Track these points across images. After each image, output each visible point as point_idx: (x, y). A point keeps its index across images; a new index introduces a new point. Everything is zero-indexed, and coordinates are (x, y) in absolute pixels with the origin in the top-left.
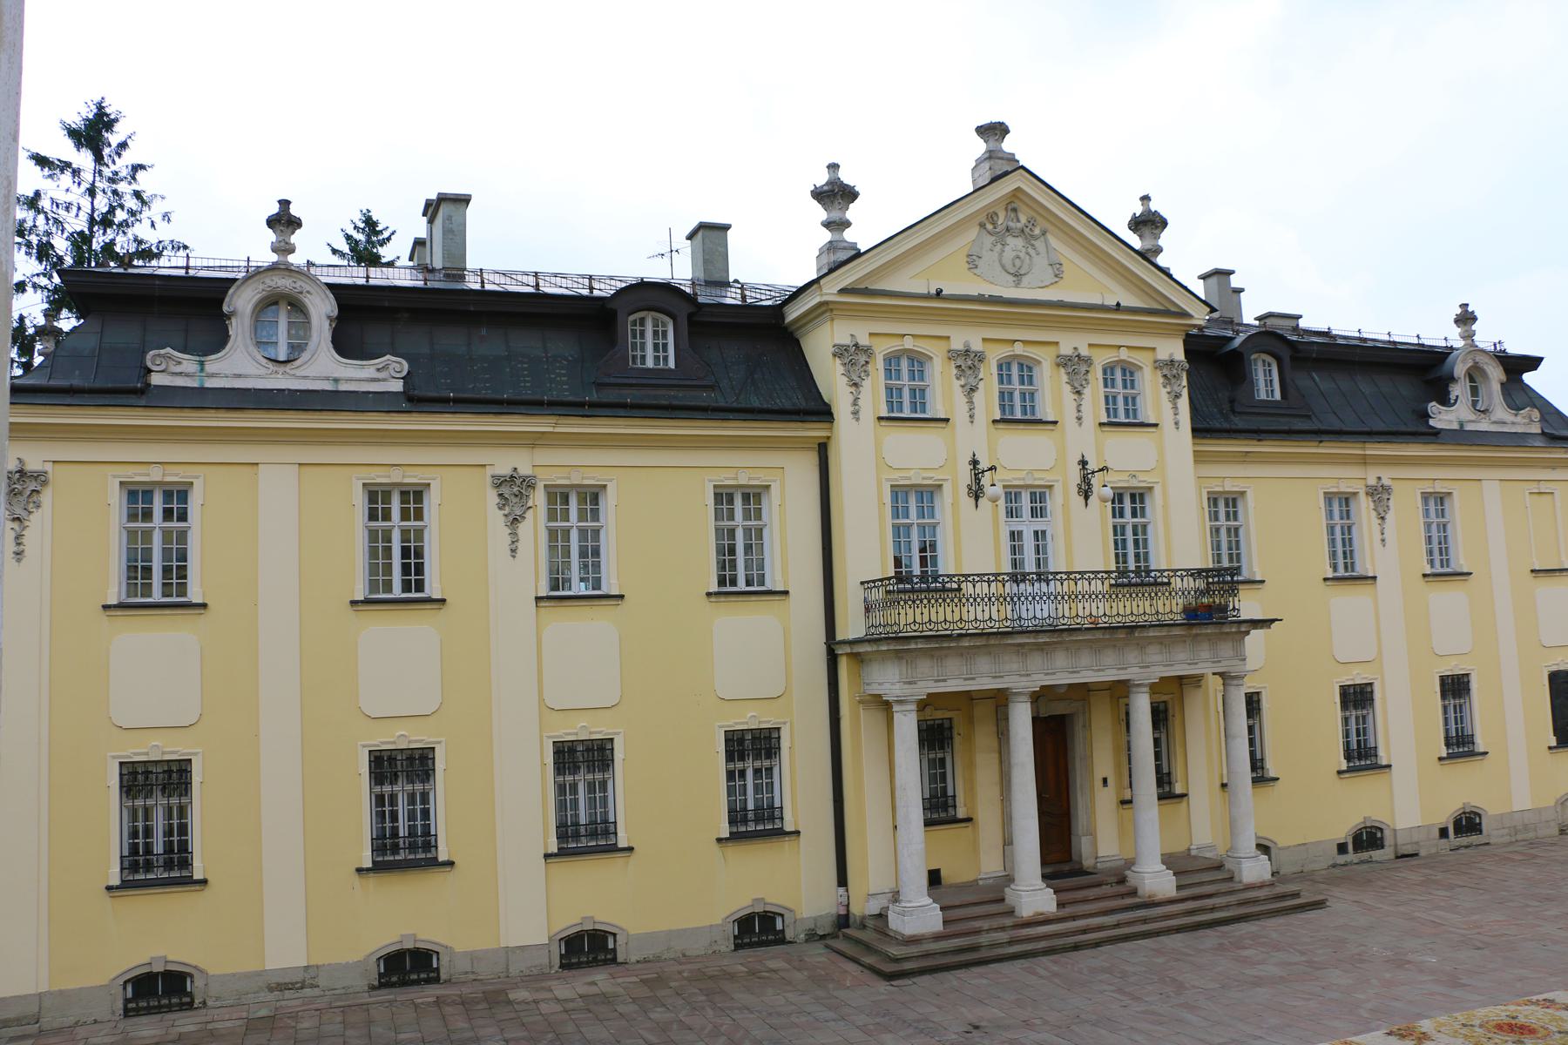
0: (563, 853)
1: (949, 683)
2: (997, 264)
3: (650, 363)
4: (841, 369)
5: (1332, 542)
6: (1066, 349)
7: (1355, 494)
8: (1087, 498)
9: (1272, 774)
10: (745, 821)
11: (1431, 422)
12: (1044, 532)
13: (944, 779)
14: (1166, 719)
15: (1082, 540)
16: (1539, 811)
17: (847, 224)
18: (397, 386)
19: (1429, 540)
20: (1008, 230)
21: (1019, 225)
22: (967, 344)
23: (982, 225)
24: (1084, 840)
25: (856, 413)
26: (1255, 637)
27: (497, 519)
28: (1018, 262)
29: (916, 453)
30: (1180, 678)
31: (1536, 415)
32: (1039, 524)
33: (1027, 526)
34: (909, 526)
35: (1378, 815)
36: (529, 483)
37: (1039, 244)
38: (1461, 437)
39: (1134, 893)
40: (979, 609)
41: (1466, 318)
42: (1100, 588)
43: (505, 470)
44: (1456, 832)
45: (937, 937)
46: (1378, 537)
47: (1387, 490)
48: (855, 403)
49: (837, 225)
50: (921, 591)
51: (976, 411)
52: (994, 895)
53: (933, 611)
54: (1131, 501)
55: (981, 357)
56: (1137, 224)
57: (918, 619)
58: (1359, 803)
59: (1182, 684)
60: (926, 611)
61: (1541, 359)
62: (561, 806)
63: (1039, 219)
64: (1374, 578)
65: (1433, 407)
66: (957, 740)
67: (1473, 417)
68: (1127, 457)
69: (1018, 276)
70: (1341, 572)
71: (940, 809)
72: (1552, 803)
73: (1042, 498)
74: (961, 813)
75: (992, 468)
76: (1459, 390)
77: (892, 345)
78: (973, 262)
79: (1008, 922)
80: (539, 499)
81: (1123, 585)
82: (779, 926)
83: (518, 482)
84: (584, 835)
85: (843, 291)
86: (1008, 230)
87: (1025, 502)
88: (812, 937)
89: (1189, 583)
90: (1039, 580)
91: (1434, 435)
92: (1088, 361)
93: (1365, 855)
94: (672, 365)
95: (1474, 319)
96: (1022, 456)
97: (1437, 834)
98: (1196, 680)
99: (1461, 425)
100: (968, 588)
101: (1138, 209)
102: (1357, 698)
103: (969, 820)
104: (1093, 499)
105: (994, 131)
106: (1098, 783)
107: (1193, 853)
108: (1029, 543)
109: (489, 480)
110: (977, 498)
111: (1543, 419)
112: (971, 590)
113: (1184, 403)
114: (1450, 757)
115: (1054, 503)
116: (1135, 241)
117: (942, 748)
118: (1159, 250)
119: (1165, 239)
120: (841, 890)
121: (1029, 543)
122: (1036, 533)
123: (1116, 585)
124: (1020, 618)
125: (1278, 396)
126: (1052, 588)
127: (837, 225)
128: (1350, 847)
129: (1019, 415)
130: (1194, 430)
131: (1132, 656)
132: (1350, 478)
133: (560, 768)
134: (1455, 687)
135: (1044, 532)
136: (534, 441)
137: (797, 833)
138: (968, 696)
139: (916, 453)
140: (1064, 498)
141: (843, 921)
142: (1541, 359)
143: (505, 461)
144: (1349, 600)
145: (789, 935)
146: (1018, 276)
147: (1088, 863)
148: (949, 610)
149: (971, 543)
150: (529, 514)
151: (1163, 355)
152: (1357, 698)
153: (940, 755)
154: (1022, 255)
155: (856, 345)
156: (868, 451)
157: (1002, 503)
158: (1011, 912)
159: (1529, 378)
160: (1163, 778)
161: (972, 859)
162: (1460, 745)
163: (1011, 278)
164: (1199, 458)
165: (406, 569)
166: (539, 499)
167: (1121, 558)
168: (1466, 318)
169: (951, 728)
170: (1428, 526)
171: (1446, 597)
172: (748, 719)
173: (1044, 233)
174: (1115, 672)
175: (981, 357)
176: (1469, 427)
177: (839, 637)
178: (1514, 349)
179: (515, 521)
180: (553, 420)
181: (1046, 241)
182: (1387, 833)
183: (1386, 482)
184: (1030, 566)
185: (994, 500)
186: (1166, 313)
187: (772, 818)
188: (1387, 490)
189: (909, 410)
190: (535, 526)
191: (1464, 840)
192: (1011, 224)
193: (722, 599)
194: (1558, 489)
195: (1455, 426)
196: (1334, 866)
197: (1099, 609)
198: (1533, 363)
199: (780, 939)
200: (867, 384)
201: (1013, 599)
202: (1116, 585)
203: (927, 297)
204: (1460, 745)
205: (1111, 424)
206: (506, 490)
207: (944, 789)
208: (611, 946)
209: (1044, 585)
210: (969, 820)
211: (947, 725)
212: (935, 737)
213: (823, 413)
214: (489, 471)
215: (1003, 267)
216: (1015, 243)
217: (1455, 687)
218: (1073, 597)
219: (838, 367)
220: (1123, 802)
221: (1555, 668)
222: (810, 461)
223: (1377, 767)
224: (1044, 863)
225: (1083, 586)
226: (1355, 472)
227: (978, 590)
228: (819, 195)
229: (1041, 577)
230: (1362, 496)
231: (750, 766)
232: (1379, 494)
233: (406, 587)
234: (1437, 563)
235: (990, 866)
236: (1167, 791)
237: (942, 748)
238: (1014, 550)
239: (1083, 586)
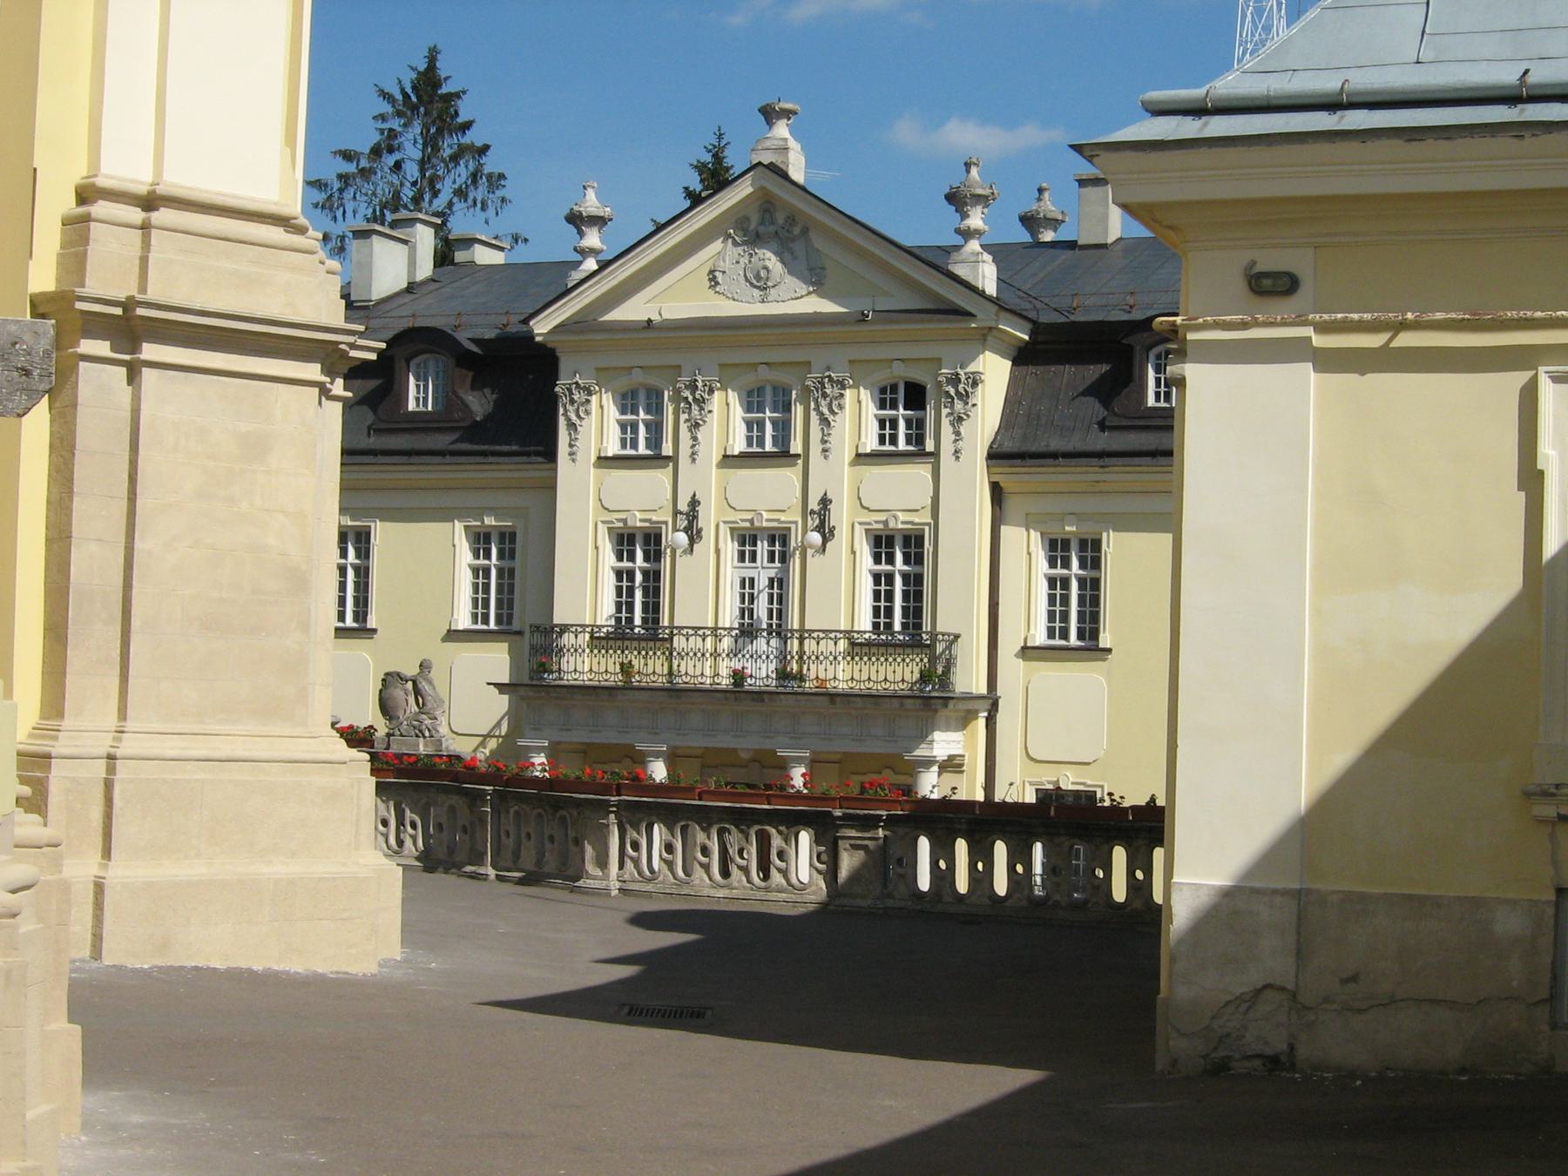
2: (742, 279)
20: (758, 235)
21: (772, 229)
28: (763, 274)
37: (798, 247)
51: (700, 448)
73: (784, 540)
87: (762, 548)
100: (680, 643)
122: (771, 580)
163: (756, 293)
173: (805, 231)
192: (761, 229)
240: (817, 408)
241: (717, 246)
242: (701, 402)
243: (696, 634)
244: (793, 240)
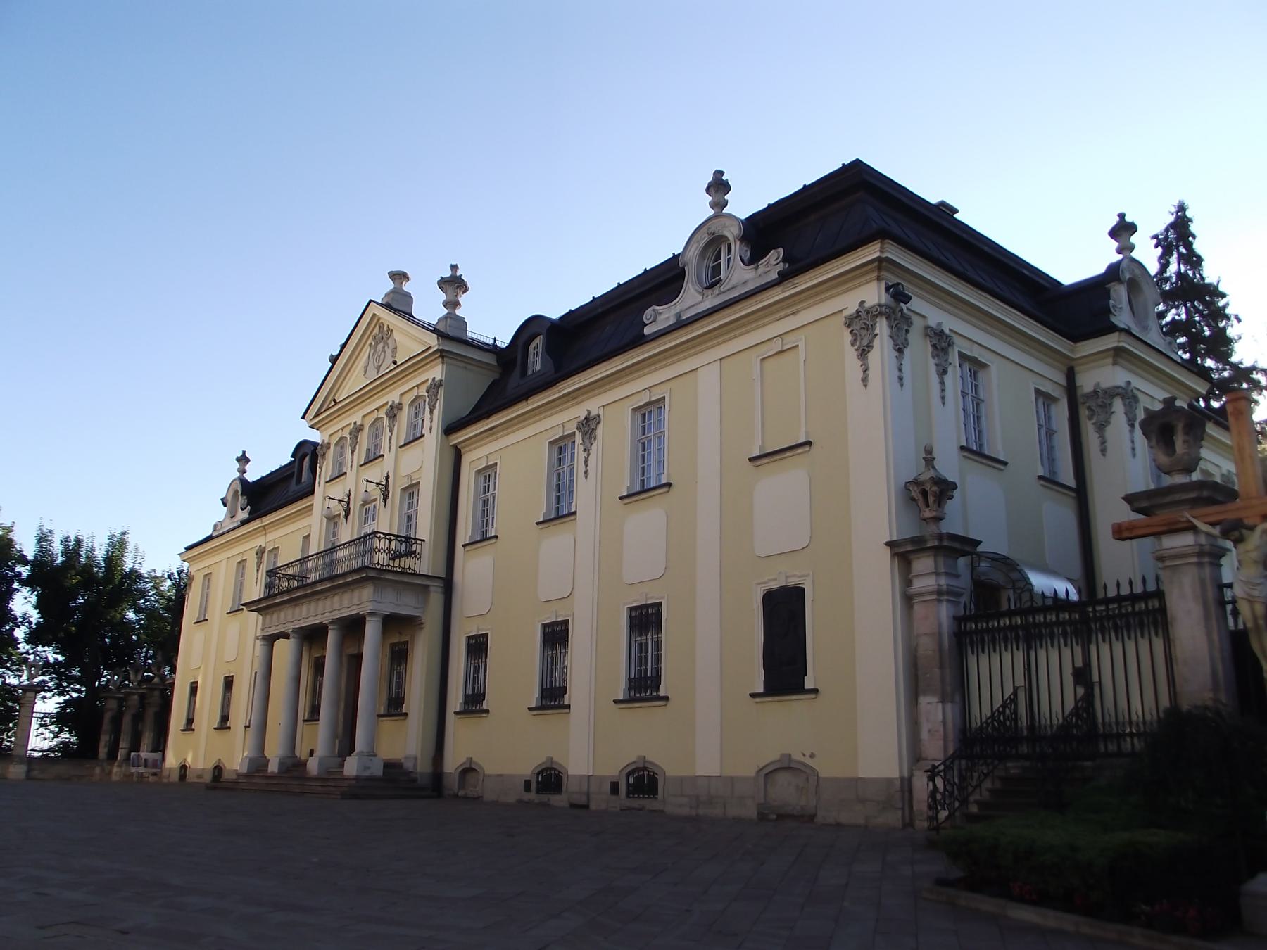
37: (389, 341)
44: (628, 794)
65: (648, 313)
72: (753, 774)
93: (544, 798)
97: (607, 788)
99: (679, 315)
129: (374, 457)
132: (566, 419)
146: (378, 368)
152: (556, 635)
162: (644, 686)
183: (594, 413)
191: (636, 803)
194: (799, 339)
196: (520, 801)
204: (644, 686)
216: (380, 347)
217: (645, 620)
221: (773, 585)
241: (366, 351)
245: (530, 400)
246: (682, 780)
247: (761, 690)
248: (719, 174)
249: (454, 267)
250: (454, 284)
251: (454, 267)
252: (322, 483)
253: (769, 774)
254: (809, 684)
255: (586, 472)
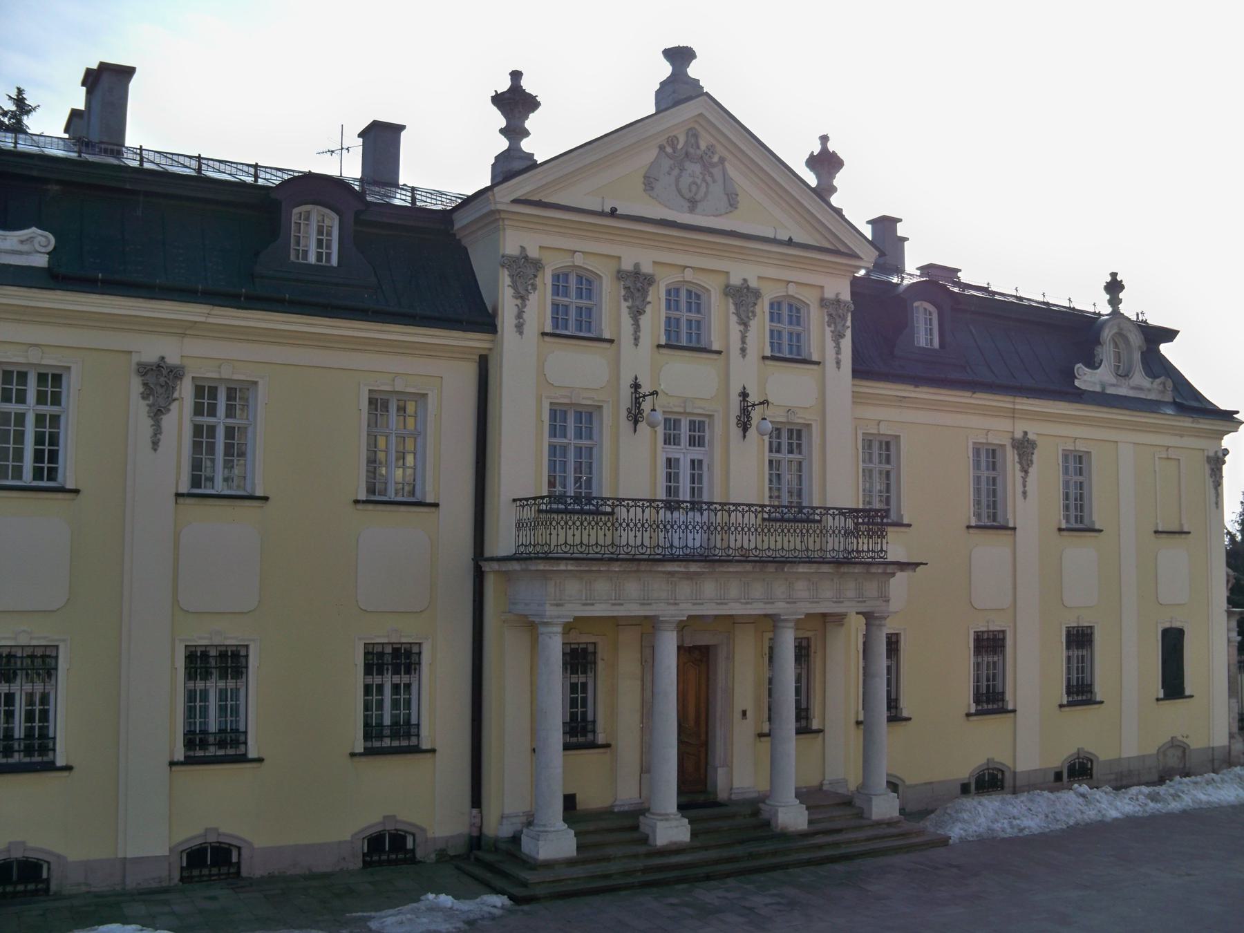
0: (189, 761)
1: (597, 607)
3: (312, 259)
4: (508, 281)
5: (978, 491)
6: (735, 280)
7: (1003, 446)
8: (745, 430)
9: (905, 714)
10: (380, 737)
11: (1077, 383)
12: (700, 462)
13: (584, 704)
14: (808, 655)
15: (742, 473)
16: (1142, 758)
17: (526, 133)
18: (41, 261)
19: (1067, 496)
20: (687, 154)
21: (699, 152)
22: (637, 265)
23: (662, 148)
24: (720, 771)
25: (519, 327)
26: (899, 581)
27: (140, 409)
28: (694, 188)
29: (580, 371)
30: (824, 615)
31: (1169, 384)
32: (696, 453)
33: (685, 454)
34: (564, 448)
35: (1002, 757)
36: (176, 374)
38: (1102, 399)
39: (767, 824)
40: (632, 534)
41: (1114, 287)
42: (753, 521)
43: (150, 357)
45: (570, 862)
46: (1019, 489)
47: (1033, 445)
48: (520, 315)
49: (514, 131)
50: (574, 512)
51: (641, 334)
52: (629, 823)
53: (585, 533)
54: (791, 439)
55: (650, 280)
56: (813, 162)
57: (570, 541)
58: (985, 744)
59: (828, 621)
60: (578, 533)
61: (1177, 332)
62: (190, 712)
63: (719, 148)
64: (1014, 529)
65: (1080, 368)
66: (600, 665)
67: (1114, 381)
68: (788, 390)
69: (693, 204)
70: (985, 521)
71: (580, 732)
74: (601, 739)
75: (654, 393)
76: (1106, 353)
77: (561, 262)
78: (649, 183)
79: (642, 849)
80: (186, 390)
81: (776, 520)
82: (410, 845)
83: (164, 372)
84: (213, 743)
85: (516, 201)
86: (687, 154)
88: (443, 857)
89: (840, 522)
90: (692, 509)
91: (1079, 396)
92: (757, 294)
94: (334, 261)
95: (1122, 287)
96: (685, 382)
97: (1052, 778)
98: (839, 619)
100: (622, 513)
101: (817, 149)
102: (990, 644)
103: (607, 746)
104: (752, 432)
105: (680, 56)
106: (737, 715)
107: (825, 788)
108: (685, 472)
109: (134, 367)
110: (636, 422)
111: (1175, 389)
112: (624, 515)
113: (847, 343)
114: (1071, 704)
115: (715, 433)
116: (812, 179)
117: (584, 672)
118: (834, 190)
119: (839, 180)
120: (475, 811)
121: (685, 472)
122: (693, 461)
123: (769, 520)
124: (672, 546)
125: (936, 344)
126: (705, 518)
127: (514, 131)
128: (973, 787)
130: (853, 371)
131: (780, 589)
133: (191, 674)
134: (1080, 639)
135: (700, 462)
136: (185, 330)
137: (433, 751)
138: (617, 623)
139: (580, 371)
140: (723, 428)
141: (476, 842)
142: (1177, 332)
143: (152, 349)
144: (990, 549)
145: (419, 854)
146: (693, 204)
147: (722, 795)
148: (601, 533)
149: (632, 466)
150: (174, 407)
151: (829, 294)
152: (990, 644)
153: (582, 679)
154: (699, 182)
155: (526, 258)
156: (532, 364)
157: (660, 430)
158: (645, 840)
159: (1165, 349)
160: (803, 714)
161: (608, 783)
164: (857, 398)
165: (38, 455)
166: (186, 390)
167: (775, 491)
168: (1114, 287)
169: (595, 653)
170: (1066, 484)
171: (1079, 552)
172: (385, 633)
173: (722, 160)
174: (761, 605)
175: (650, 280)
176: (1110, 391)
177: (487, 554)
178: (1153, 321)
179: (157, 413)
180: (204, 309)
181: (724, 173)
182: (1007, 774)
184: (685, 495)
185: (653, 425)
186: (837, 252)
187: (408, 735)
188: (1033, 445)
189: (574, 325)
190: (180, 418)
192: (691, 151)
193: (370, 507)
195: (1098, 389)
197: (750, 542)
198: (1170, 335)
199: (411, 859)
200: (533, 298)
201: (667, 527)
202: (769, 520)
203: (602, 214)
205: (773, 358)
206: (151, 379)
207: (584, 714)
208: (234, 859)
209: (698, 515)
210: (607, 746)
211: (591, 649)
212: (579, 660)
213: (486, 322)
214: (135, 359)
215: (679, 191)
218: (726, 528)
219: (505, 279)
220: (761, 735)
222: (470, 371)
223: (1004, 711)
224: (680, 792)
225: (736, 518)
226: (1004, 425)
227: (632, 515)
228: (498, 100)
229: (695, 506)
230: (1009, 449)
231: (388, 680)
232: (1025, 447)
233: (38, 474)
234: (1072, 520)
235: (627, 794)
236: (804, 728)
237: (584, 672)
238: (669, 477)
239: (736, 518)
240: (737, 314)
242: (644, 293)
243: (650, 506)
244: (714, 165)
245: (977, 395)
246: (1111, 762)
247: (1161, 695)
248: (1114, 275)
249: (824, 139)
250: (826, 162)
251: (824, 139)
252: (532, 328)
253: (1162, 751)
254: (1187, 693)
255: (1024, 493)
